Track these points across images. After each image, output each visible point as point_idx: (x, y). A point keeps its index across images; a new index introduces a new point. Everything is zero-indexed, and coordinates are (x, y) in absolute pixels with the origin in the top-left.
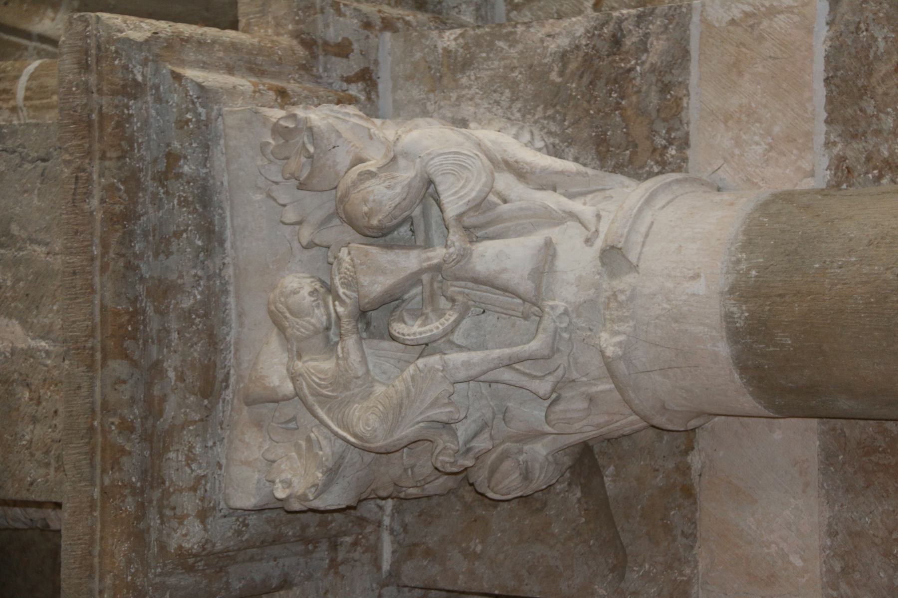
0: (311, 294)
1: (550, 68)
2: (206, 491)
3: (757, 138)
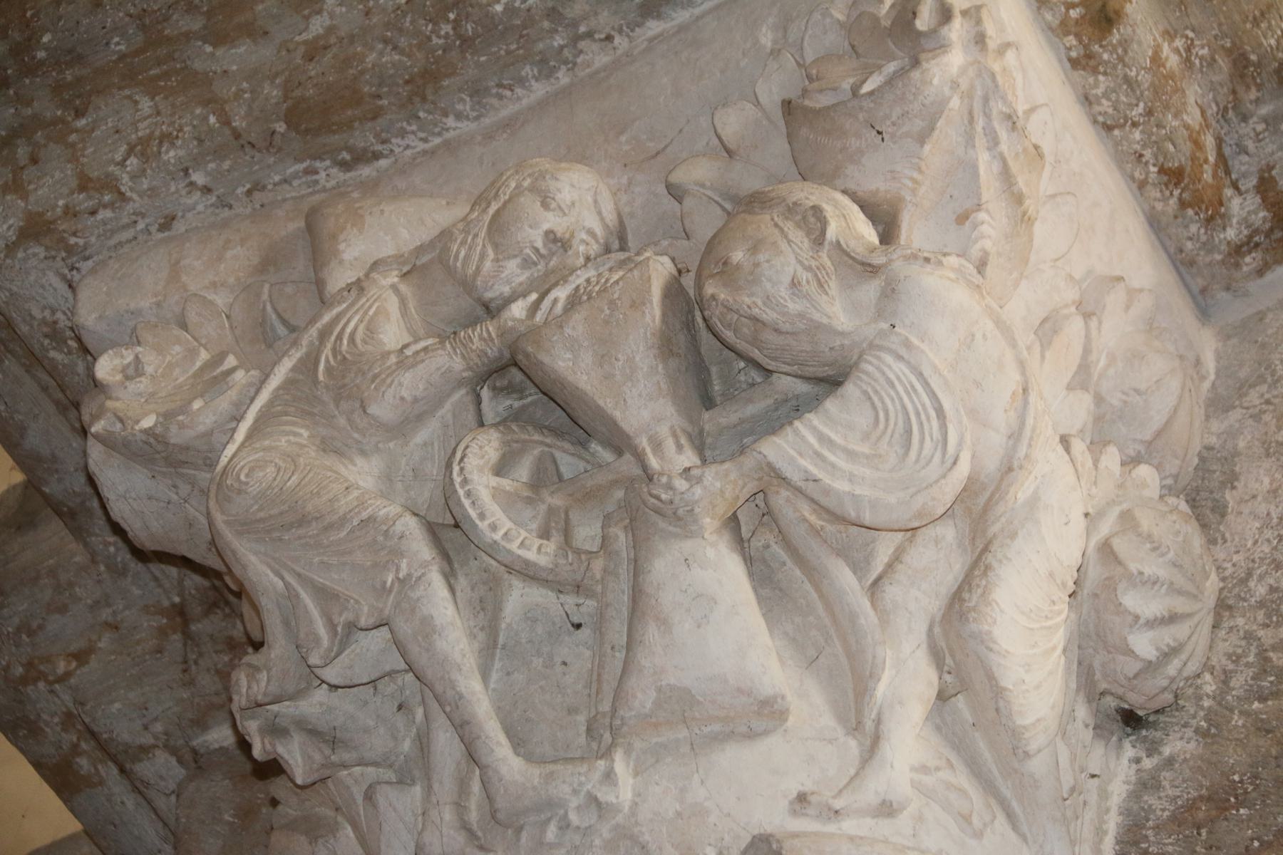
0: (551, 236)
2: (93, 213)
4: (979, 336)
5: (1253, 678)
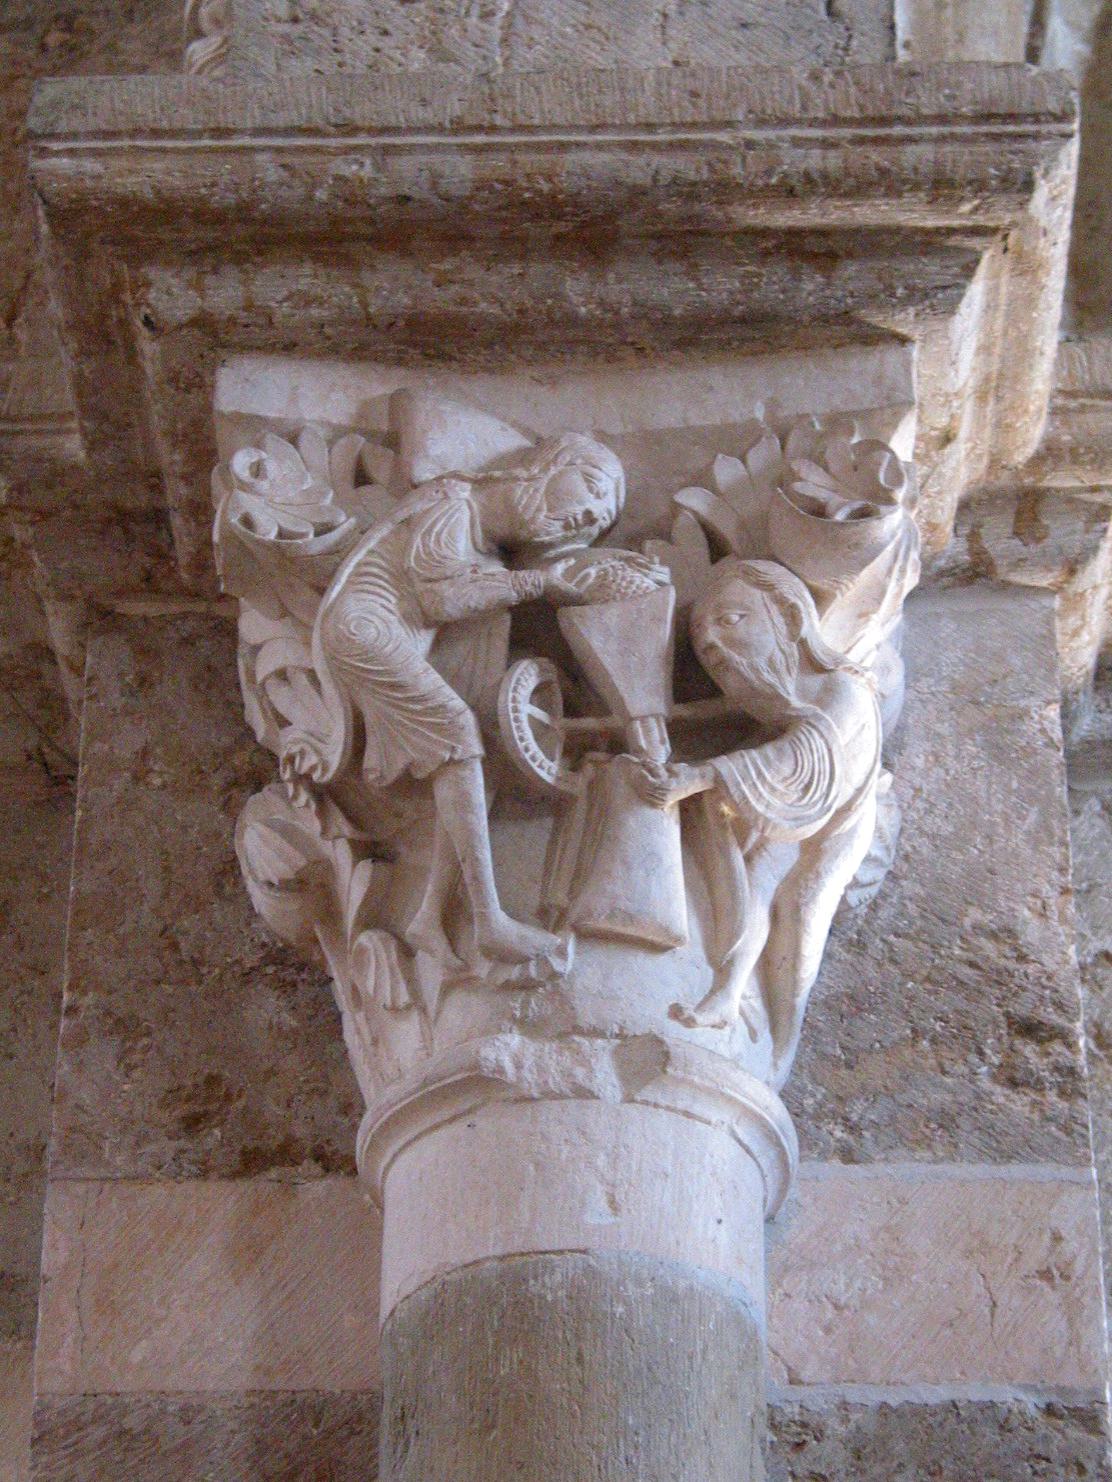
0: (588, 514)
1: (988, 907)
3: (858, 1284)
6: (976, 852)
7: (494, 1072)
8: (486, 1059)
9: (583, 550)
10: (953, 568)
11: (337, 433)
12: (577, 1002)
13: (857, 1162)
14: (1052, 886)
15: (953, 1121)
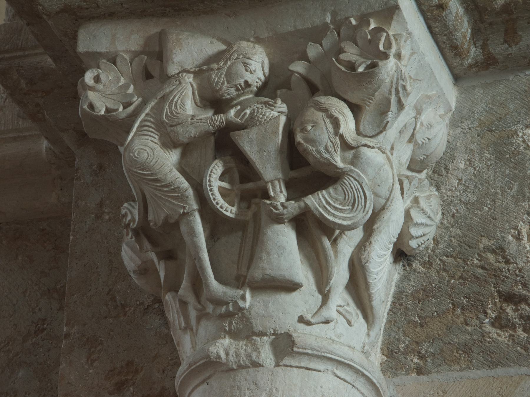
0: (246, 82)
1: (492, 237)
4: (382, 171)
5: (446, 247)
6: (487, 209)
7: (216, 358)
8: (212, 352)
9: (250, 98)
10: (476, 63)
11: (136, 55)
12: (253, 320)
13: (424, 374)
14: (524, 222)
15: (470, 349)
